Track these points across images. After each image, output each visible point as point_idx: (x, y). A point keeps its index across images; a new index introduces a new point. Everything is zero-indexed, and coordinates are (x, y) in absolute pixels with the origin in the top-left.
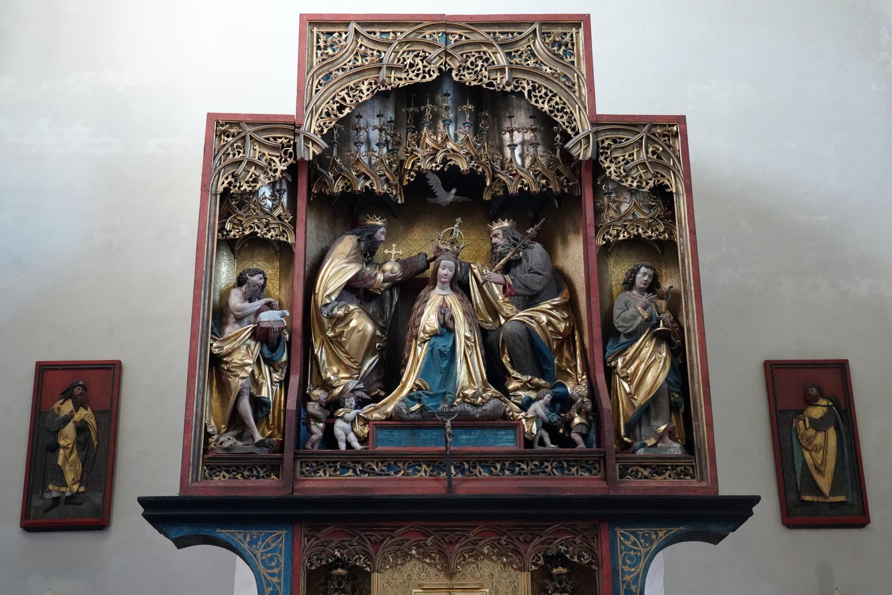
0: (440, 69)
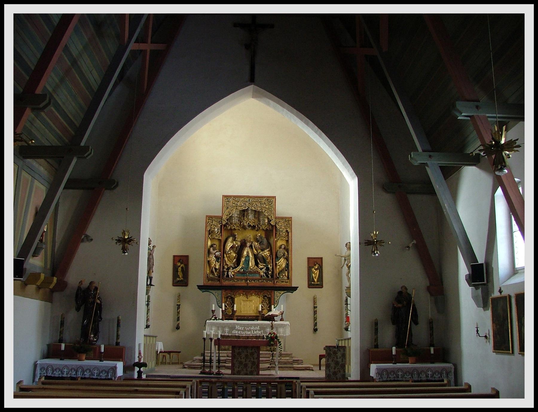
0: (248, 207)
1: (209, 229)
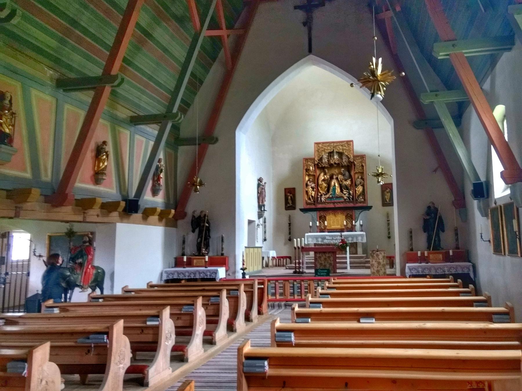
1: (306, 167)
